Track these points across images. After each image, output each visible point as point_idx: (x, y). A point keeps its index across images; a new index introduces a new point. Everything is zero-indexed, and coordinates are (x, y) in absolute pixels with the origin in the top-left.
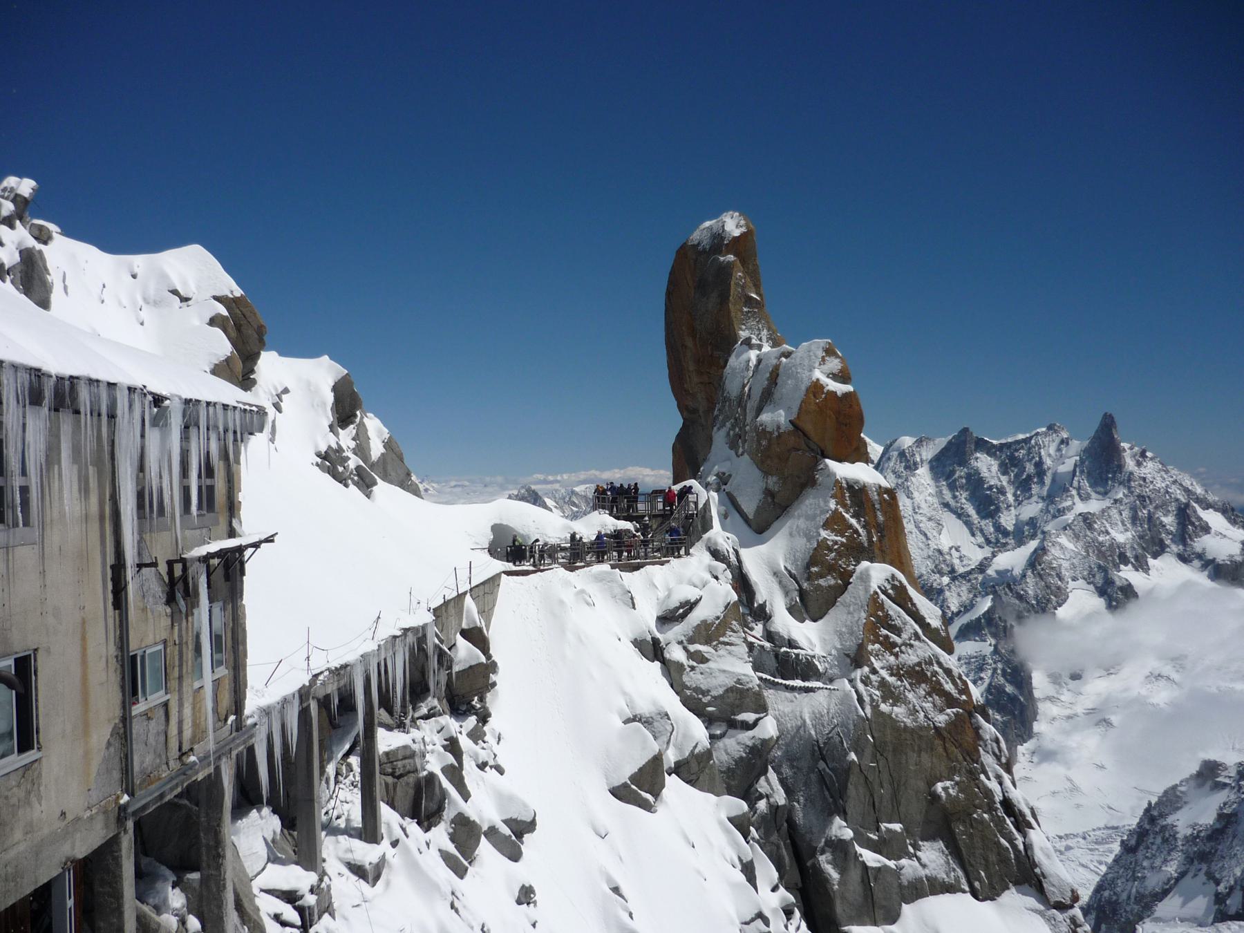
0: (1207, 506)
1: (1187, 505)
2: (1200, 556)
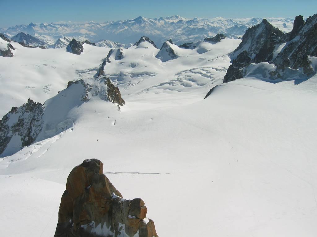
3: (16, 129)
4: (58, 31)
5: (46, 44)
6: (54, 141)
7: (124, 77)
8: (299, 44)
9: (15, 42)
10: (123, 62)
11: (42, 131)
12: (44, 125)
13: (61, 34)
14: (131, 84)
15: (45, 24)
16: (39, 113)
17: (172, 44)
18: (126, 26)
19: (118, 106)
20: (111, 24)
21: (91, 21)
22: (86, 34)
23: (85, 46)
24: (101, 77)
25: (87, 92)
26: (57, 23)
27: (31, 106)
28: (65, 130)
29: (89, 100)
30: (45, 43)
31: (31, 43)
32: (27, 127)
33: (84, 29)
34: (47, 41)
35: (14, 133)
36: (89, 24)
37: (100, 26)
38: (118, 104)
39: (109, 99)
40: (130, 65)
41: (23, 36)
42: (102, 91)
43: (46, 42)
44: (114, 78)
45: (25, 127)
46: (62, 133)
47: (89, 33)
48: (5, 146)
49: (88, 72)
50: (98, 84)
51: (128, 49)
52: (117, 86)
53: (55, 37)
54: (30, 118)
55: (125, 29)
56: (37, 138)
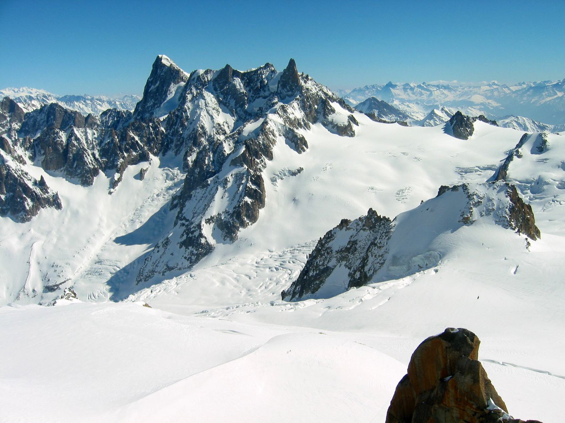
3: (344, 257)
4: (432, 97)
5: (410, 118)
6: (402, 287)
7: (545, 187)
9: (361, 112)
10: (546, 159)
11: (384, 265)
12: (389, 257)
13: (437, 101)
14: (557, 201)
15: (412, 85)
16: (384, 234)
18: (560, 91)
19: (526, 239)
20: (531, 87)
21: (493, 81)
22: (482, 104)
23: (478, 125)
24: (500, 182)
25: (471, 208)
26: (431, 83)
27: (373, 220)
28: (423, 271)
29: (474, 222)
30: (408, 116)
31: (386, 115)
32: (362, 255)
33: (479, 94)
34: (412, 114)
35: (339, 262)
36: (489, 85)
37: (509, 89)
38: (526, 236)
39: (511, 225)
40: (560, 164)
41: (374, 104)
42: (500, 209)
43: (411, 114)
44: (525, 187)
45: (357, 254)
46: (417, 274)
47: (487, 101)
48: (322, 282)
49: (479, 173)
50: (494, 194)
51: (558, 134)
52: (530, 203)
53: (426, 108)
54: (368, 240)
55: (555, 97)
56: (374, 277)
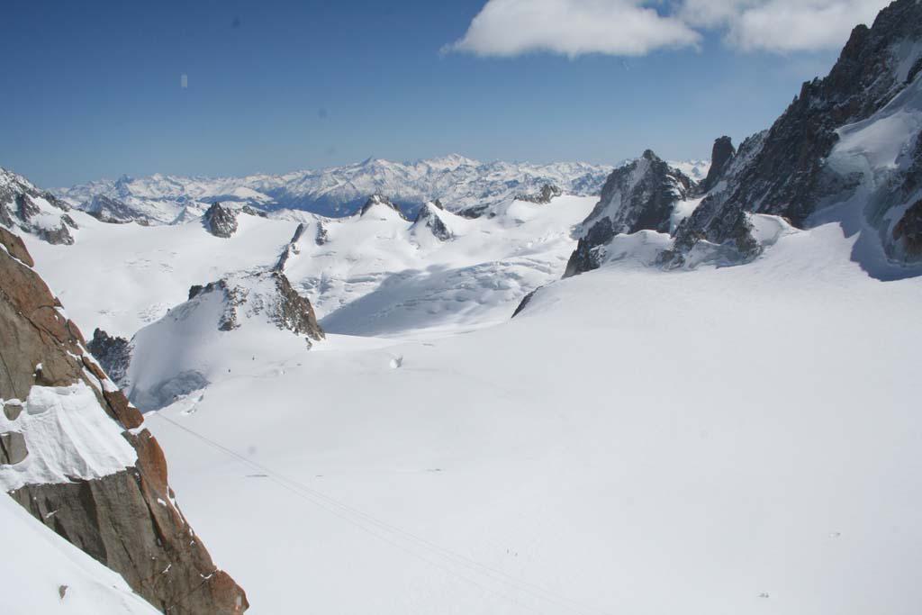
0: (35, 195)
1: (23, 196)
2: (35, 227)
8: (727, 198)
17: (441, 208)
